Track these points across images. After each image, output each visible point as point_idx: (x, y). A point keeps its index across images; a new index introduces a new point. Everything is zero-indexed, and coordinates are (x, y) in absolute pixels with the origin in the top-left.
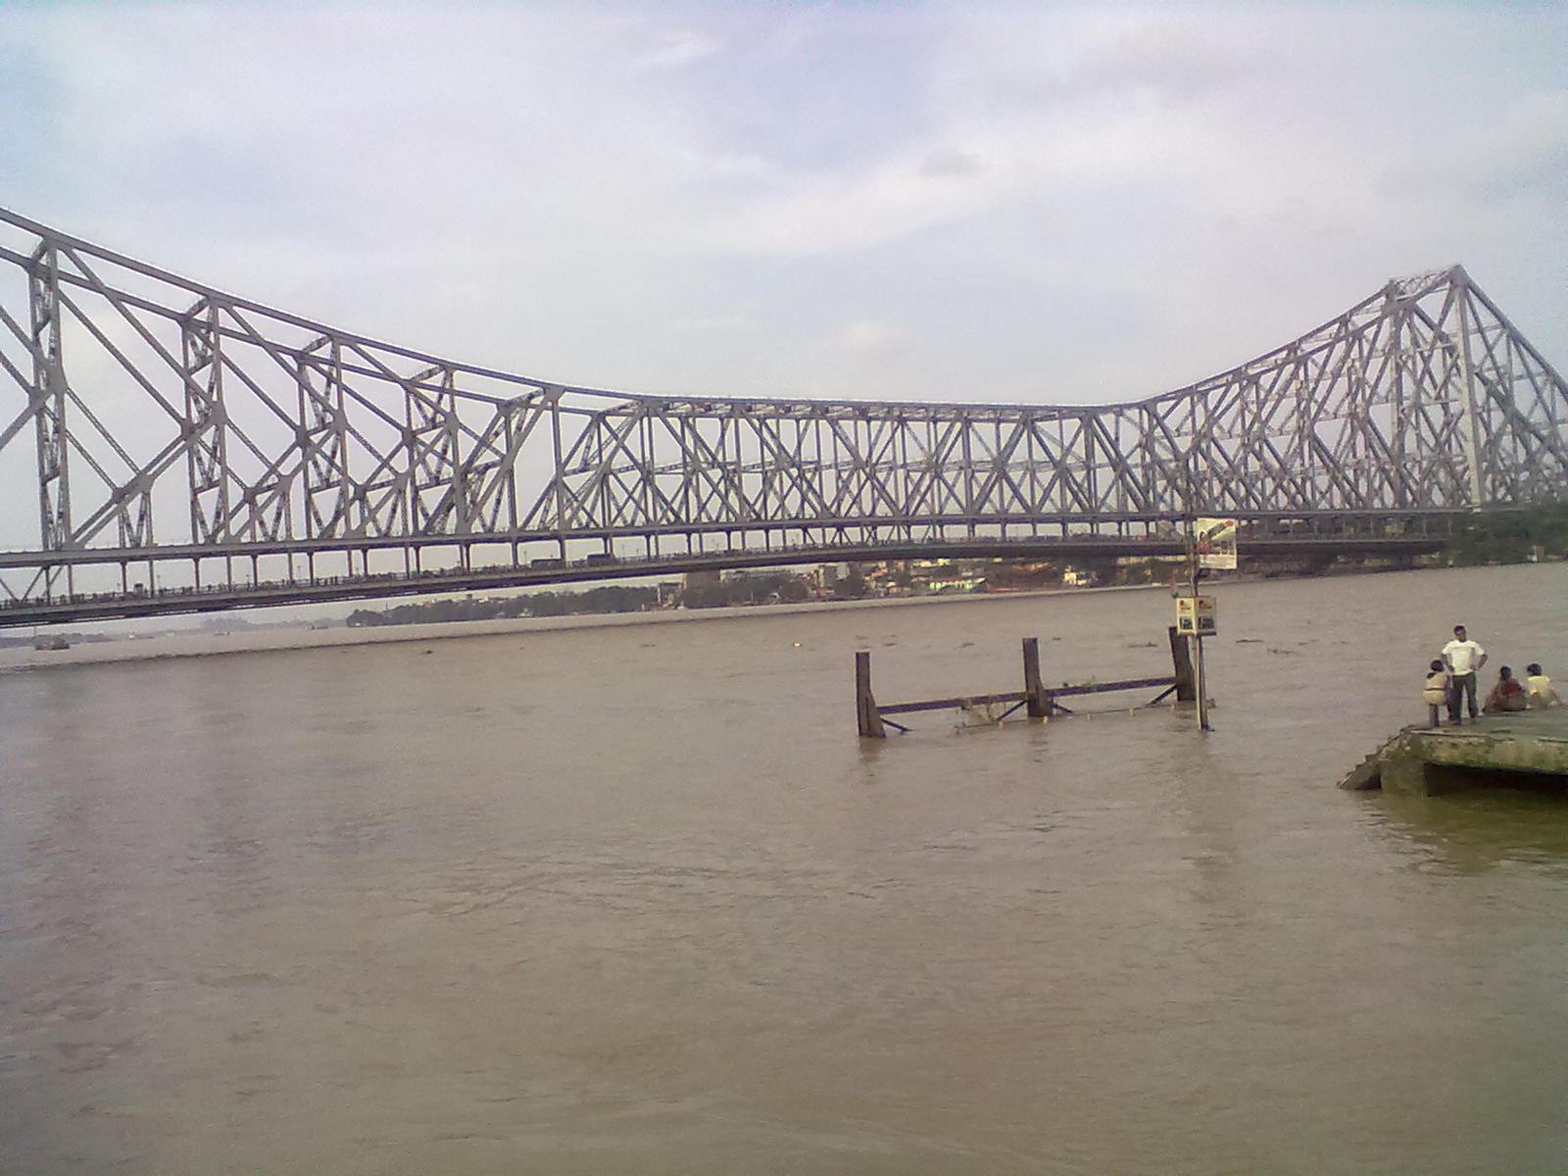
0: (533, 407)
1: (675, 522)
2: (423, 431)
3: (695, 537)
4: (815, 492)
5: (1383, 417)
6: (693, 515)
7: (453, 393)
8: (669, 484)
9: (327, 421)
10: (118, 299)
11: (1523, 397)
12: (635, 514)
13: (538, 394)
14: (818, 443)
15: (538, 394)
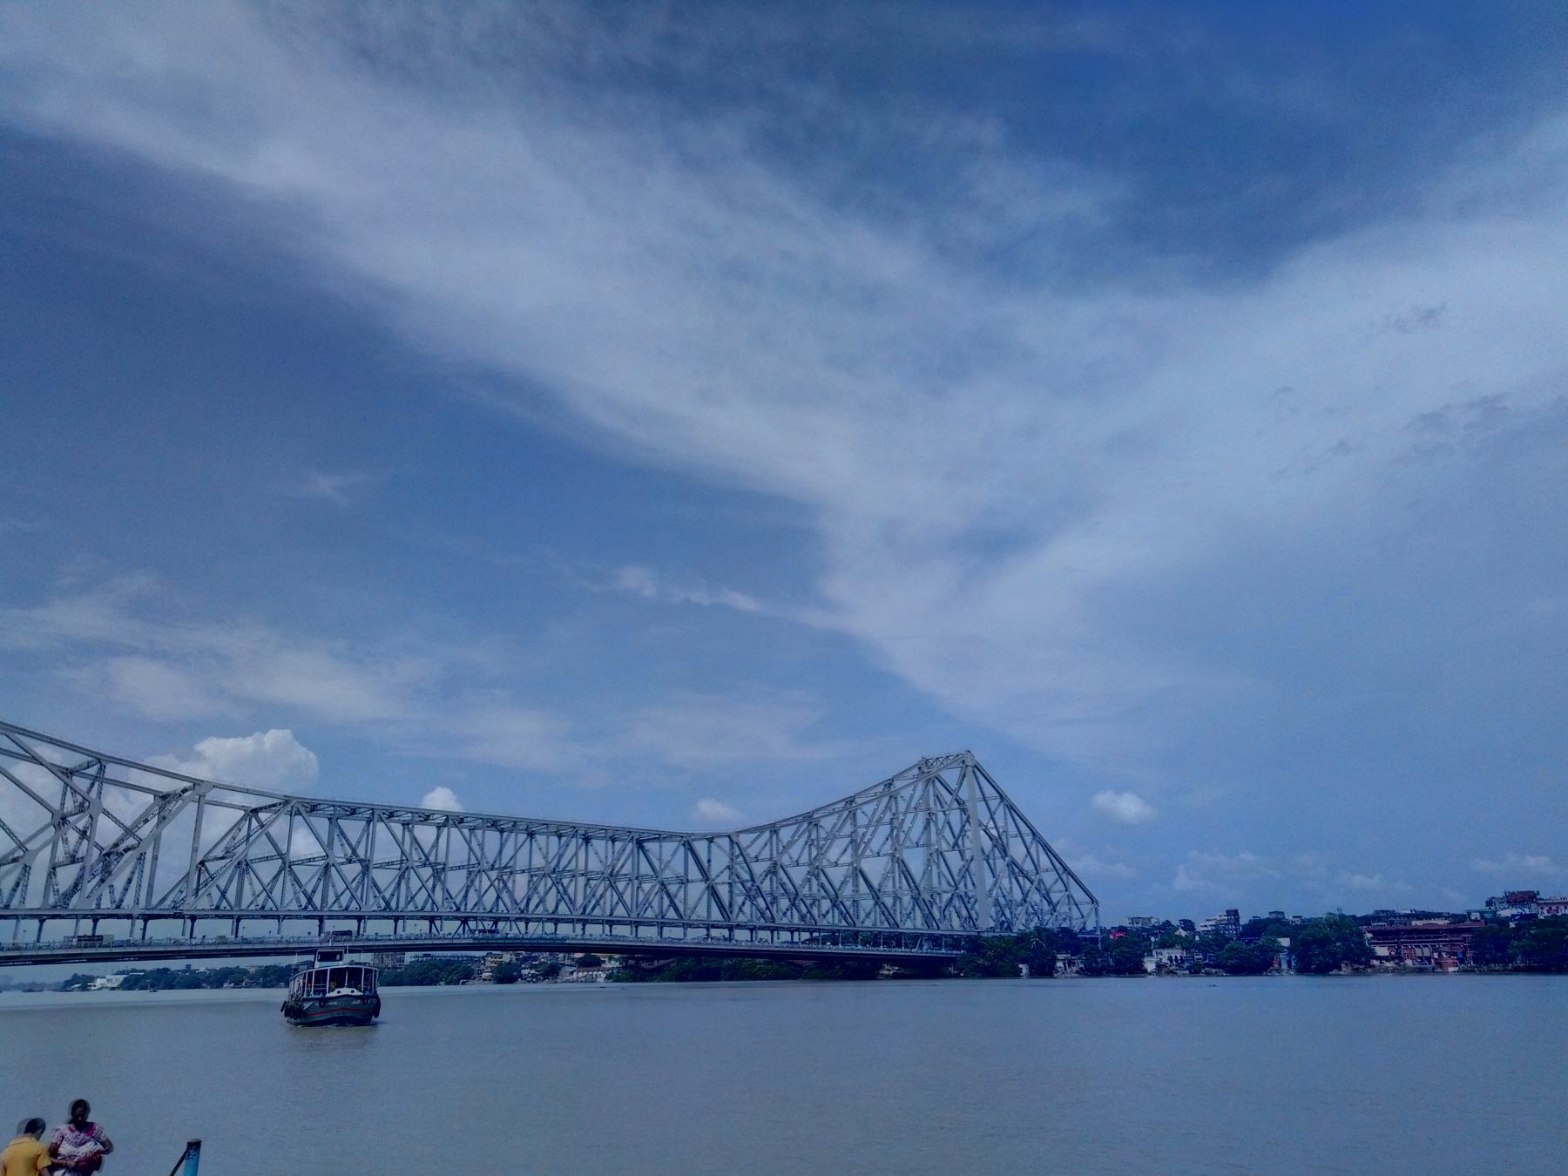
1: (385, 909)
3: (400, 922)
4: (508, 891)
5: (916, 862)
8: (384, 878)
11: (1017, 850)
12: (350, 901)
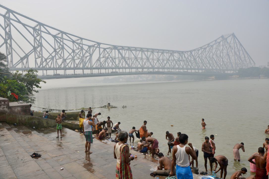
0: (95, 47)
2: (76, 50)
6: (106, 66)
7: (82, 44)
9: (60, 47)
10: (24, 25)
13: (96, 44)
14: (127, 54)
15: (96, 44)
